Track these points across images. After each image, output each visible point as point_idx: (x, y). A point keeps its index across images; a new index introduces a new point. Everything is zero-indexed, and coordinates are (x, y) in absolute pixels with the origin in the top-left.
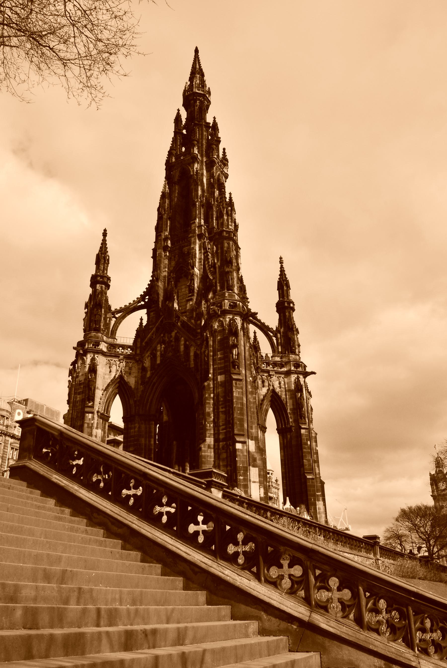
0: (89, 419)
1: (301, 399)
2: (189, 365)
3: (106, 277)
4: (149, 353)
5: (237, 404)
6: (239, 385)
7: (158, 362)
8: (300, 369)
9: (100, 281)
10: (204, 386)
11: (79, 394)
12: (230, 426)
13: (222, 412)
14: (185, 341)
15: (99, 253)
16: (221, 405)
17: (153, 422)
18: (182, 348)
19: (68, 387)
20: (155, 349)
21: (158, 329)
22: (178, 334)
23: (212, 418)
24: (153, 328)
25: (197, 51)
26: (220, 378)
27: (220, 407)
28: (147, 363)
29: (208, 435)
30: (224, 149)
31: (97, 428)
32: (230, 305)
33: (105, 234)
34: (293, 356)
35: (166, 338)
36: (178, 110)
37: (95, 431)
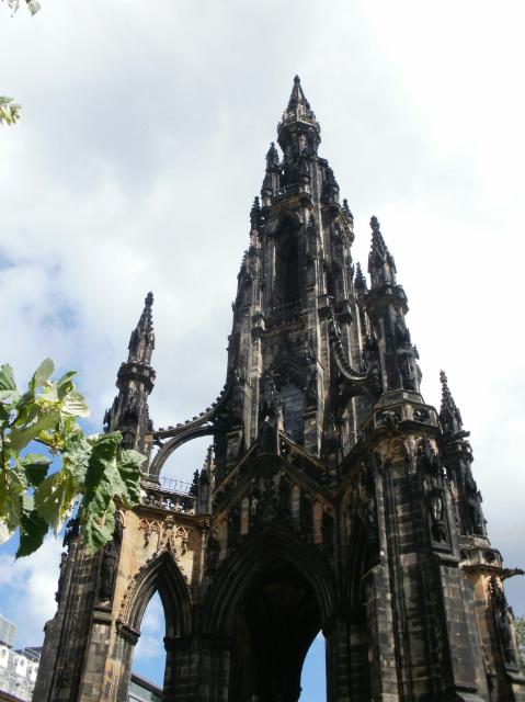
0: (101, 635)
1: (504, 621)
2: (312, 539)
3: (147, 368)
4: (225, 513)
5: (452, 617)
6: (454, 574)
7: (244, 530)
8: (495, 564)
9: (136, 375)
10: (372, 575)
11: (82, 581)
12: (438, 666)
13: (415, 633)
14: (303, 492)
15: (137, 330)
16: (413, 617)
17: (229, 653)
18: (296, 505)
19: (61, 566)
20: (238, 507)
21: (243, 469)
22: (286, 479)
23: (393, 646)
24: (234, 467)
25: (297, 80)
26: (406, 560)
27: (410, 622)
28: (221, 533)
29: (385, 686)
30: (345, 201)
31: (114, 656)
32: (415, 414)
33: (149, 300)
34: (480, 540)
35: (262, 486)
36: (273, 144)
37: (109, 661)
